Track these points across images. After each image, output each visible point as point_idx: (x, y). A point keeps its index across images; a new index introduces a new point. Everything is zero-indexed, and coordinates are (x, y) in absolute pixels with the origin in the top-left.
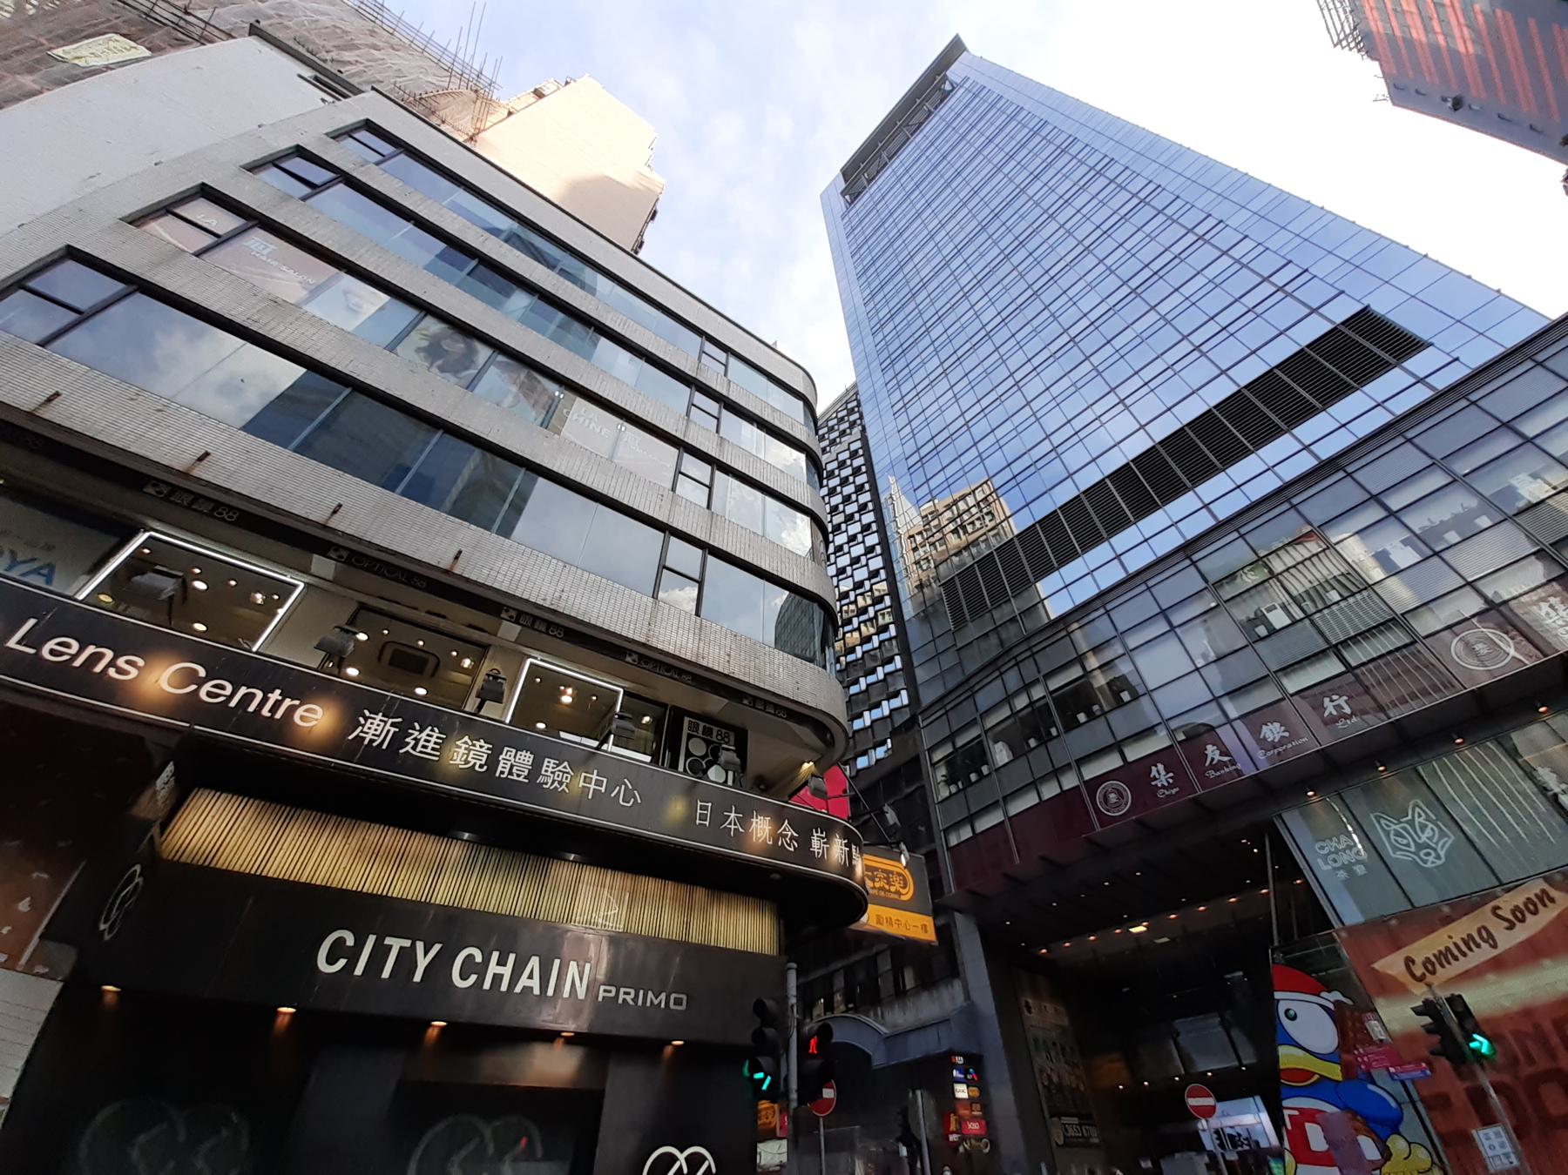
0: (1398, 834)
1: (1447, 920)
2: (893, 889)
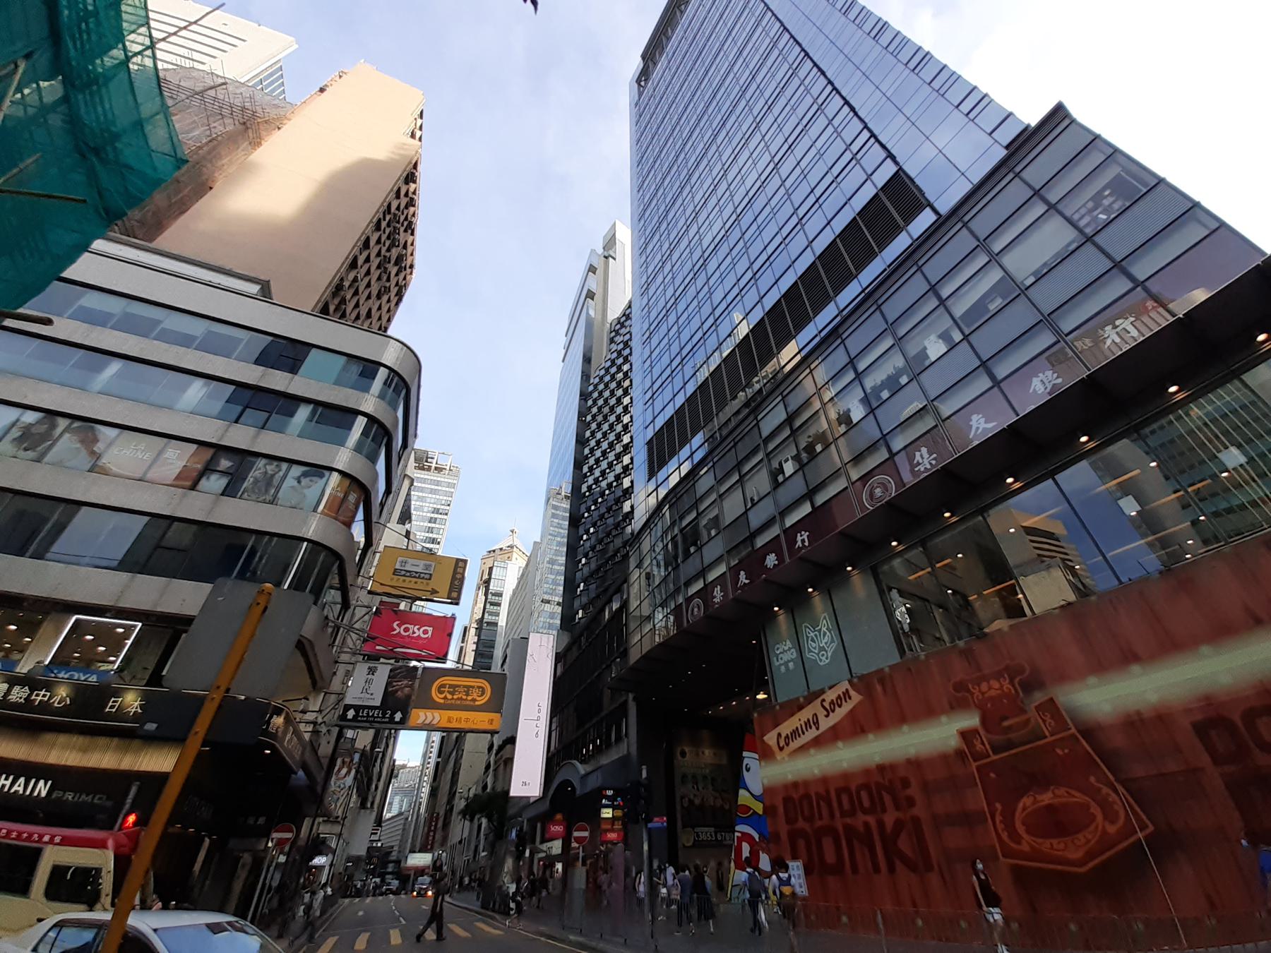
1: (801, 708)
2: (469, 698)
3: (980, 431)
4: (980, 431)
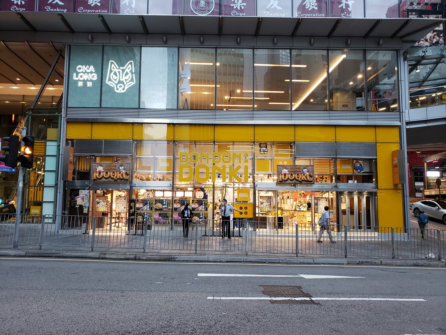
0: (115, 74)
3: (273, 7)
4: (273, 7)
